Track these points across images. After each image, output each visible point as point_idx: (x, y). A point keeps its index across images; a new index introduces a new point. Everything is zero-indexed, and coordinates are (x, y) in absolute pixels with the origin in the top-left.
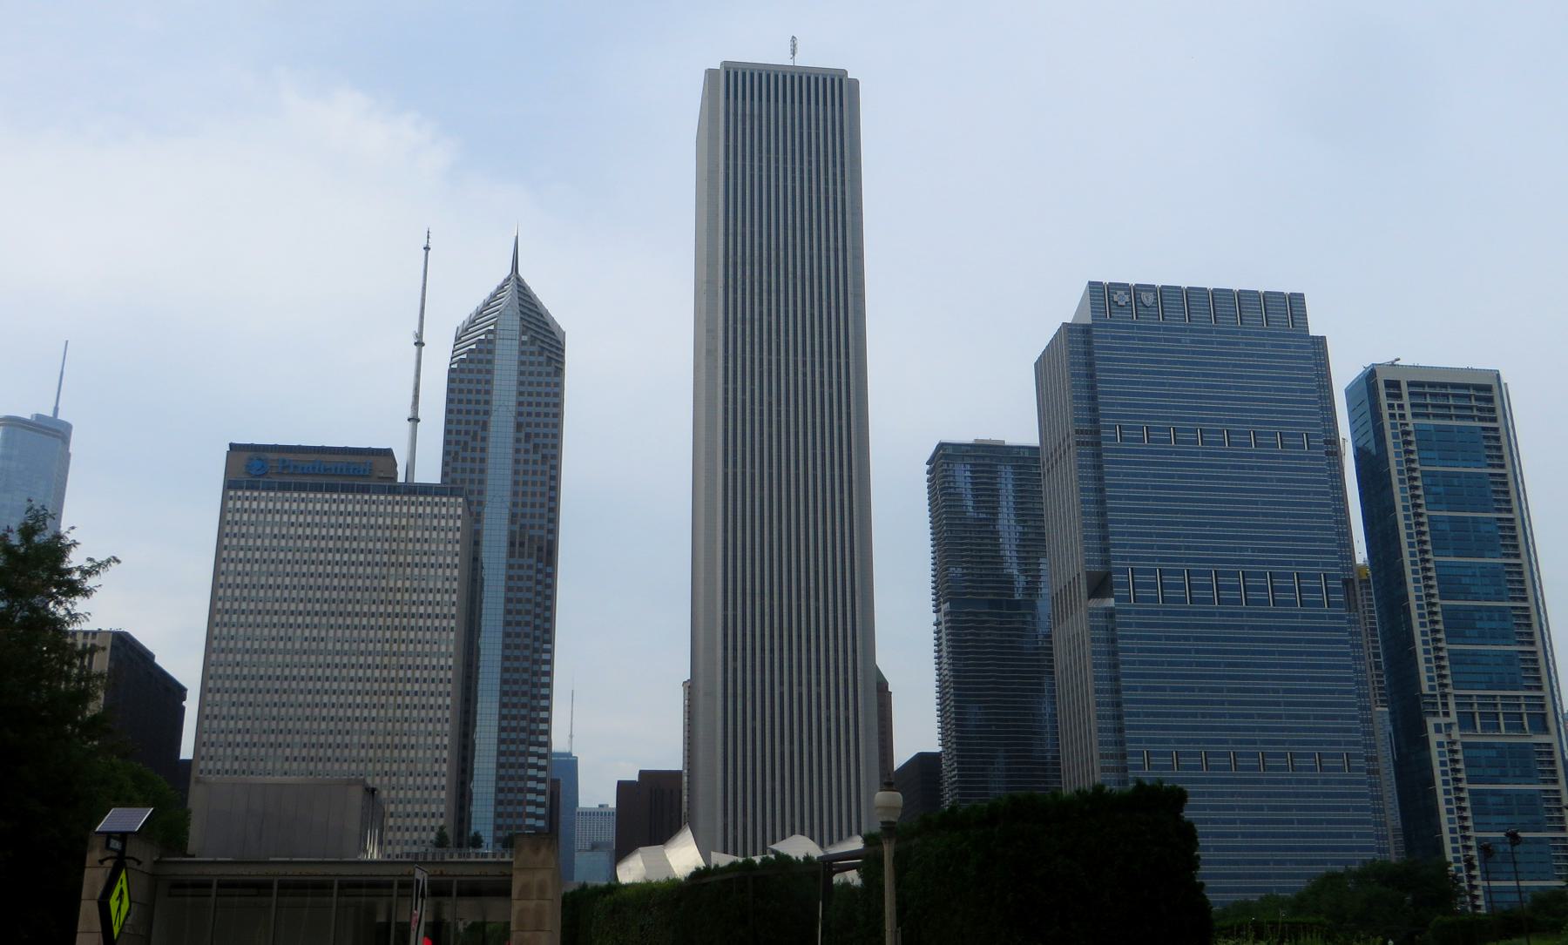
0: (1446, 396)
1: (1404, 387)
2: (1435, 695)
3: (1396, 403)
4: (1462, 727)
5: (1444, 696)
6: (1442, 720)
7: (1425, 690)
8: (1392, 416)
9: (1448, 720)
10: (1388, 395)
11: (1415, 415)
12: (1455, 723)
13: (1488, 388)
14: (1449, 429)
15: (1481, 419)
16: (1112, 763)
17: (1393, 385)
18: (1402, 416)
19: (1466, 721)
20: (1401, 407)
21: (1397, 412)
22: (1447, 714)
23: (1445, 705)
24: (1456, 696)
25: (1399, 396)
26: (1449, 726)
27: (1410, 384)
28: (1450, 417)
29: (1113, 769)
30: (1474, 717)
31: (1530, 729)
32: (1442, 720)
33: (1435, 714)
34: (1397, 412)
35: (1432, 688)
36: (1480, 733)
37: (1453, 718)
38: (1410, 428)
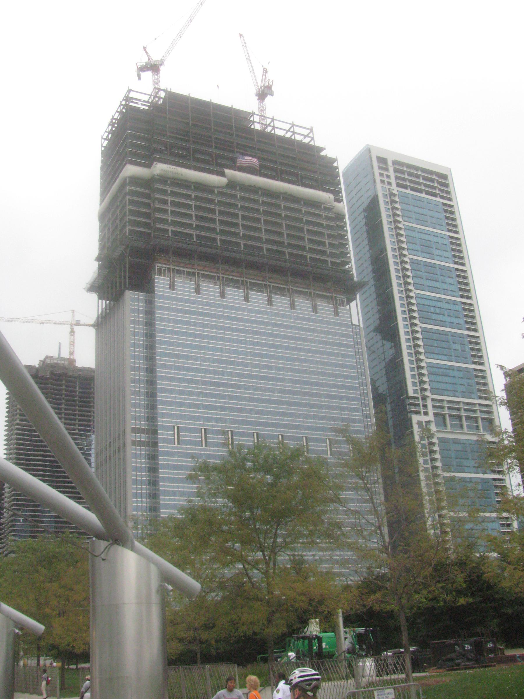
0: (418, 177)
1: (390, 163)
2: (417, 398)
3: (385, 173)
4: (436, 425)
5: (424, 398)
6: (423, 418)
7: (411, 393)
8: (382, 182)
9: (426, 419)
10: (380, 168)
11: (398, 185)
12: (432, 421)
13: (445, 177)
14: (421, 200)
15: (442, 197)
16: (143, 438)
17: (382, 161)
18: (389, 184)
19: (440, 418)
20: (388, 177)
21: (386, 180)
22: (426, 414)
23: (425, 406)
24: (433, 400)
25: (387, 170)
26: (429, 422)
27: (395, 163)
28: (420, 191)
29: (143, 444)
30: (444, 419)
31: (483, 430)
32: (423, 418)
33: (418, 413)
34: (386, 180)
35: (415, 391)
36: (449, 430)
37: (431, 417)
38: (395, 192)
